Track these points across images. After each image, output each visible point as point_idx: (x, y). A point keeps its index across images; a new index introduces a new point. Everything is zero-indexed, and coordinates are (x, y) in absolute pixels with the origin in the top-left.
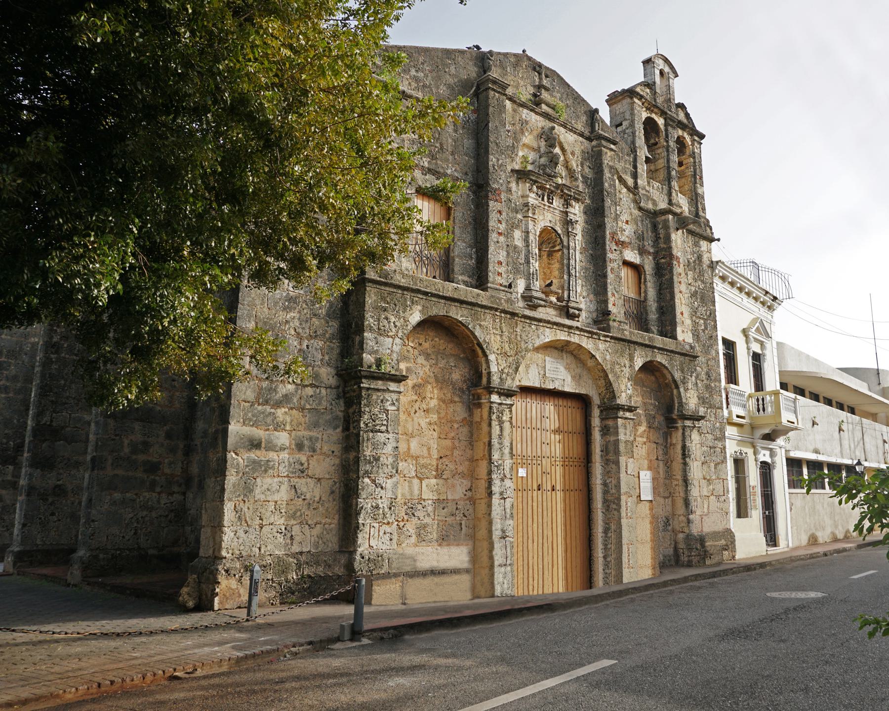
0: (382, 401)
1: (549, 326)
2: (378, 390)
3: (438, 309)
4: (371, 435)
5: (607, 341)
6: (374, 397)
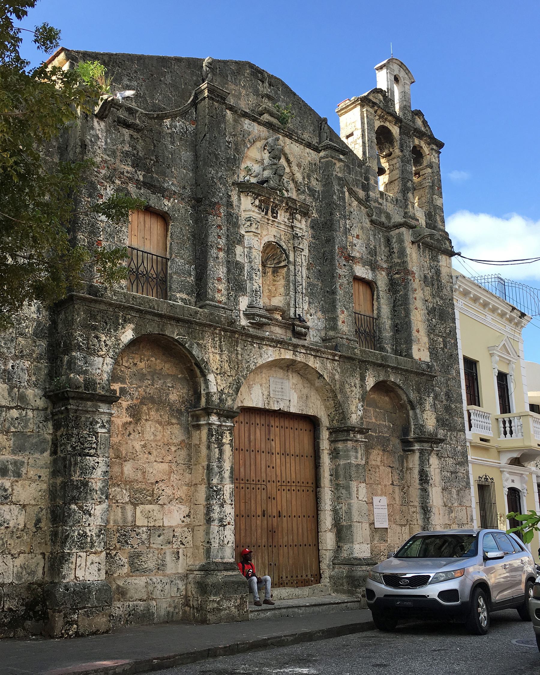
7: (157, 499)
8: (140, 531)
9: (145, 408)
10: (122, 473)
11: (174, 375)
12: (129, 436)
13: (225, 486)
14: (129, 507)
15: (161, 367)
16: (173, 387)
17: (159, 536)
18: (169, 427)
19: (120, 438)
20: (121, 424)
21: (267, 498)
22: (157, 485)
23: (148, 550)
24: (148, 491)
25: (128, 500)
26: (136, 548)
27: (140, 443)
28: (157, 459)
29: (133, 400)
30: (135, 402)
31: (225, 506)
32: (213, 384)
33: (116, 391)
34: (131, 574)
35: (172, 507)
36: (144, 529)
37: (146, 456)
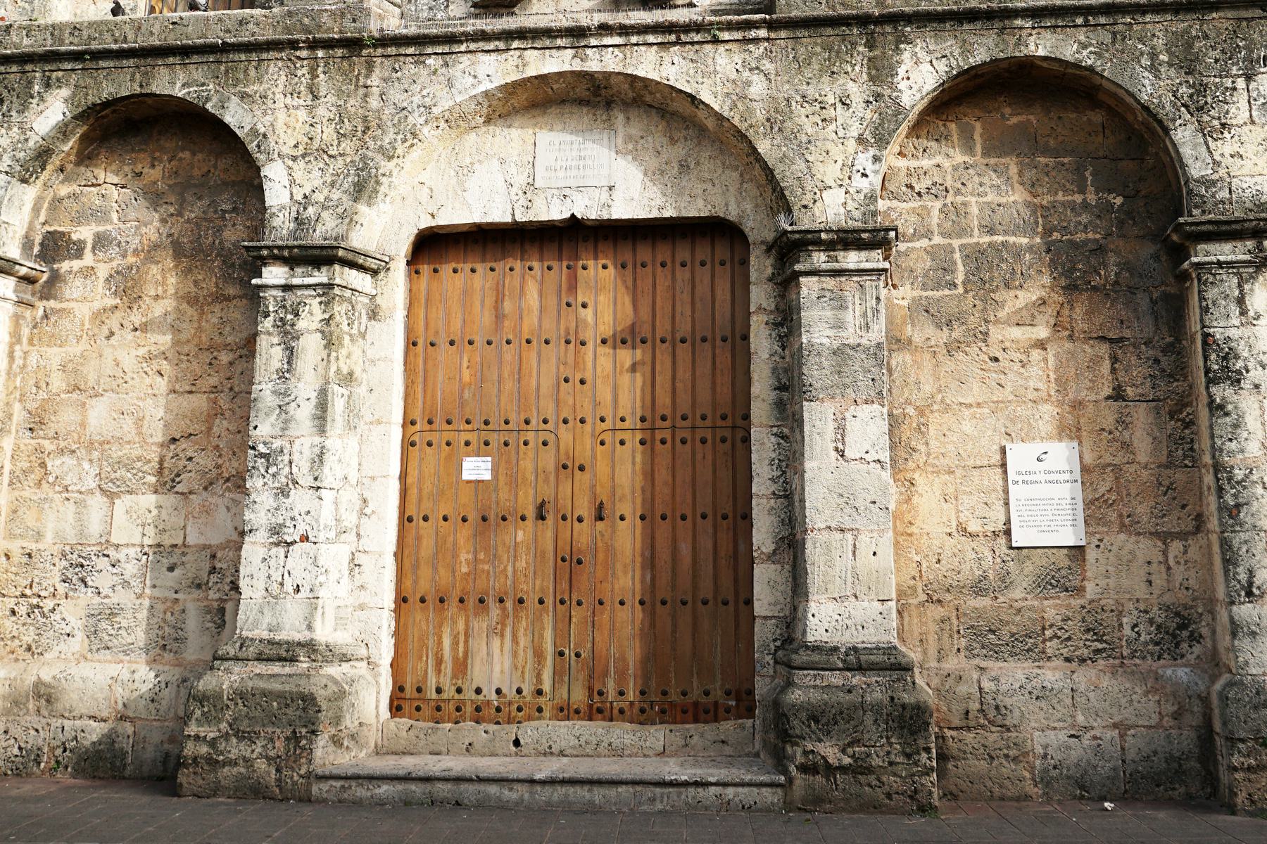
1: (491, 46)
5: (756, 40)
7: (173, 481)
8: (121, 556)
9: (154, 269)
10: (83, 425)
11: (242, 181)
12: (108, 338)
13: (297, 442)
14: (98, 501)
15: (205, 169)
16: (235, 209)
17: (171, 569)
18: (217, 308)
19: (84, 345)
21: (556, 469)
22: (172, 447)
24: (149, 461)
25: (93, 485)
26: (107, 597)
27: (134, 353)
28: (177, 387)
29: (124, 256)
30: (131, 259)
31: (292, 492)
34: (89, 656)
35: (213, 500)
37: (148, 381)
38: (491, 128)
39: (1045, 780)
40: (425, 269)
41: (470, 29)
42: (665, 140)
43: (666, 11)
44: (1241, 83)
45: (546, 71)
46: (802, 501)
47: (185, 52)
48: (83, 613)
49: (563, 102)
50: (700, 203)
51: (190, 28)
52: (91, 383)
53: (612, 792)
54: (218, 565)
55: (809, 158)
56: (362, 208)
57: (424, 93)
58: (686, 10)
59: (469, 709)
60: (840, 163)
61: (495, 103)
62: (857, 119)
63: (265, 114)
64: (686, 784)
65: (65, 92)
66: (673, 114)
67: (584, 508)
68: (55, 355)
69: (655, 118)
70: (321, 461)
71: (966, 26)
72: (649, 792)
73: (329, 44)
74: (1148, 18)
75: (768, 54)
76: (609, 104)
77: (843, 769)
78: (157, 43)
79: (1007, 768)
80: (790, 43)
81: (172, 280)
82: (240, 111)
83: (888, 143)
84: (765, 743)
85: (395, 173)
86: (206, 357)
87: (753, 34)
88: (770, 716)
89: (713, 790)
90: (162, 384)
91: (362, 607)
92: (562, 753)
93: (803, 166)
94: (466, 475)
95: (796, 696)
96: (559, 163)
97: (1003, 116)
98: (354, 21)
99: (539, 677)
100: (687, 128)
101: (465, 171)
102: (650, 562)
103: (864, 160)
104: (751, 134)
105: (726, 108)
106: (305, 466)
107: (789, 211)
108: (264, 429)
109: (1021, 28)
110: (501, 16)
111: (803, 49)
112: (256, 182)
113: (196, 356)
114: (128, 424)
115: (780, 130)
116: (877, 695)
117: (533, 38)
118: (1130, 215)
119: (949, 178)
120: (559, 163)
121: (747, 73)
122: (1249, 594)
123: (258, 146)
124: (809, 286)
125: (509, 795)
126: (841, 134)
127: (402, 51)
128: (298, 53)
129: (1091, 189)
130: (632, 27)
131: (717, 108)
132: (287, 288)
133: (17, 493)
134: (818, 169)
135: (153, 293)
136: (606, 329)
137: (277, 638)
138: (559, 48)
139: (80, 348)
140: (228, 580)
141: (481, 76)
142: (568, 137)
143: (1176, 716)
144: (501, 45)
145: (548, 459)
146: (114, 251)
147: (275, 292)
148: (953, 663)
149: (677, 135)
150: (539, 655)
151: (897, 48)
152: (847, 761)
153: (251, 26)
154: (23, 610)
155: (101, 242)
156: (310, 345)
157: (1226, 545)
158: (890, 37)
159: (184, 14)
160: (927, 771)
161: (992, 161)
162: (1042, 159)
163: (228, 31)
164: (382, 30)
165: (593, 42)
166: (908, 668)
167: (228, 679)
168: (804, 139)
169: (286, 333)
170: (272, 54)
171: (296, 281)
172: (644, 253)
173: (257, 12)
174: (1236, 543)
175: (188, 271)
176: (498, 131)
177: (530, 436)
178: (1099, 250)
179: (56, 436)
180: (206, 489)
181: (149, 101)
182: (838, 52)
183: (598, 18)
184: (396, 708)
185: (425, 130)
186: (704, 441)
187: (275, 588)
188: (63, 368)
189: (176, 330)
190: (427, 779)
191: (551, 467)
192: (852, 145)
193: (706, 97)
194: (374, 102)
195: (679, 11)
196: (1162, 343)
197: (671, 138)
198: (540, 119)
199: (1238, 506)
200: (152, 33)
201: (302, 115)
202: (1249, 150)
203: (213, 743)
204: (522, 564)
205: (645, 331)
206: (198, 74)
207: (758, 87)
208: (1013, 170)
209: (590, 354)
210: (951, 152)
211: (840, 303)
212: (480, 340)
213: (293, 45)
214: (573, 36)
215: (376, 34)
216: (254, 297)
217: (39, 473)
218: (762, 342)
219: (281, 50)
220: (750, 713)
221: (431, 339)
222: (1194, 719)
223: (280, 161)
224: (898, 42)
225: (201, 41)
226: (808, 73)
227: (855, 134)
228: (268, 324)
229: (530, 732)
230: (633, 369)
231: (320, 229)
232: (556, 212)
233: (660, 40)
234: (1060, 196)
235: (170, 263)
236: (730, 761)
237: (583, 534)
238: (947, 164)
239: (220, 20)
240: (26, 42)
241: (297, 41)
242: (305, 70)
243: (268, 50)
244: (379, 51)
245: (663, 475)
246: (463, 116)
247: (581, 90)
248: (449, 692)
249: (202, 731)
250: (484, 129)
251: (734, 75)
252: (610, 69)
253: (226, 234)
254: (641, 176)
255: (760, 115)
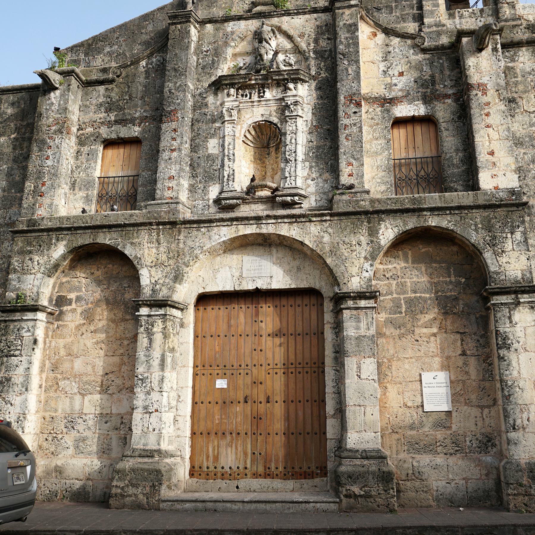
0: (18, 330)
1: (225, 224)
2: (15, 321)
3: (85, 239)
4: (5, 359)
6: (12, 327)
7: (107, 389)
8: (87, 418)
9: (99, 309)
10: (72, 368)
11: (132, 276)
12: (81, 335)
13: (153, 374)
14: (78, 397)
15: (118, 271)
16: (129, 286)
17: (106, 423)
18: (123, 324)
20: (74, 327)
21: (251, 383)
22: (106, 376)
23: (94, 435)
24: (97, 382)
25: (77, 391)
26: (82, 433)
27: (91, 341)
29: (87, 304)
30: (90, 306)
31: (152, 393)
32: (145, 277)
33: (72, 299)
34: (75, 456)
35: (122, 396)
36: (91, 416)
37: (97, 352)
38: (226, 255)
39: (437, 500)
40: (201, 308)
41: (217, 217)
42: (291, 259)
43: (292, 210)
44: (509, 235)
45: (246, 233)
46: (345, 395)
47: (110, 227)
48: (73, 440)
49: (253, 244)
50: (305, 282)
51: (112, 218)
52: (75, 353)
53: (273, 506)
54: (124, 421)
55: (346, 265)
56: (177, 285)
57: (200, 242)
58: (299, 210)
59: (219, 475)
60: (358, 267)
61: (227, 245)
62: (364, 250)
63: (140, 250)
64: (301, 502)
65: (64, 243)
66: (294, 249)
67: (262, 398)
68: (61, 342)
69: (288, 250)
70: (163, 381)
71: (405, 215)
72: (287, 505)
73: (164, 224)
74: (474, 211)
75: (330, 226)
76: (270, 245)
77: (361, 496)
78: (99, 224)
79: (423, 495)
80: (338, 221)
81: (105, 313)
82: (131, 249)
83: (376, 259)
84: (331, 486)
85: (189, 272)
86: (119, 342)
87: (324, 218)
88: (333, 476)
89: (312, 504)
90: (102, 353)
91: (178, 436)
92: (255, 491)
93: (344, 268)
94: (217, 386)
95: (343, 469)
96: (252, 268)
97: (419, 248)
98: (174, 215)
99: (245, 462)
100: (300, 254)
101: (216, 271)
102: (287, 418)
103: (367, 266)
104: (324, 256)
105: (314, 246)
106: (156, 383)
107: (339, 285)
108: (141, 369)
109: (426, 215)
110: (229, 212)
111: (343, 224)
112: (137, 276)
113: (115, 342)
114: (89, 368)
115: (335, 254)
116: (374, 468)
117: (241, 221)
118: (467, 285)
119: (399, 272)
120: (252, 268)
121: (322, 233)
122: (514, 428)
123: (138, 262)
124: (346, 314)
125: (235, 507)
126: (358, 256)
127: (192, 226)
128: (152, 227)
129: (453, 276)
130: (279, 216)
131: (311, 246)
132: (149, 316)
133: (47, 395)
134: (350, 269)
135: (98, 318)
136: (270, 331)
137: (146, 448)
138: (251, 224)
139: (71, 339)
140: (128, 427)
141: (222, 235)
142: (255, 258)
143: (487, 475)
144: (229, 223)
145: (248, 380)
146: (83, 303)
147: (144, 318)
148: (402, 456)
149: (296, 257)
150: (245, 454)
151: (379, 223)
152: (362, 493)
153: (134, 217)
154: (50, 439)
155: (79, 299)
156: (158, 338)
157: (505, 410)
158: (376, 219)
159: (109, 213)
160: (393, 497)
161: (415, 266)
162: (434, 265)
163: (126, 219)
164: (184, 218)
165: (264, 222)
166: (385, 458)
167: (128, 464)
168: (344, 258)
169: (149, 333)
170: (143, 228)
171: (152, 313)
172: (284, 301)
173: (137, 211)
174: (509, 409)
175: (111, 310)
176: (228, 256)
177: (242, 371)
178: (456, 299)
179: (62, 373)
180: (119, 392)
181: (96, 246)
182: (357, 225)
183: (266, 213)
184: (191, 475)
185: (201, 256)
186: (307, 373)
187: (145, 430)
188: (65, 347)
189: (107, 332)
190: (204, 501)
191: (249, 383)
192: (362, 260)
193: (307, 242)
194: (181, 245)
195: (297, 210)
196: (480, 334)
197: (294, 258)
198: (244, 251)
199: (509, 395)
200: (97, 220)
201: (154, 250)
202: (512, 261)
203: (122, 489)
204: (239, 420)
205: (285, 331)
206: (115, 235)
207: (327, 239)
208: (423, 269)
209: (264, 340)
210: (400, 262)
211: (358, 320)
212: (222, 335)
213: (151, 224)
214: (256, 220)
215: (182, 220)
216: (136, 319)
217: (55, 387)
218: (329, 335)
219: (146, 226)
220: (325, 475)
221: (204, 335)
222: (494, 476)
223: (146, 268)
224: (379, 221)
225: (116, 223)
226: (345, 233)
227: (364, 256)
228: (142, 329)
229: (242, 483)
230: (280, 345)
231: (161, 294)
232: (251, 286)
233: (289, 221)
234: (441, 279)
235: (105, 307)
236: (318, 493)
237: (262, 408)
238: (398, 267)
239: (123, 215)
240: (49, 224)
241: (152, 223)
242: (155, 234)
243: (141, 226)
244: (183, 226)
245: (292, 385)
246: (215, 250)
247: (260, 240)
248: (212, 468)
249: (118, 484)
250: (223, 255)
251: (317, 234)
252: (270, 232)
253: (126, 296)
254: (282, 272)
255: (327, 249)
